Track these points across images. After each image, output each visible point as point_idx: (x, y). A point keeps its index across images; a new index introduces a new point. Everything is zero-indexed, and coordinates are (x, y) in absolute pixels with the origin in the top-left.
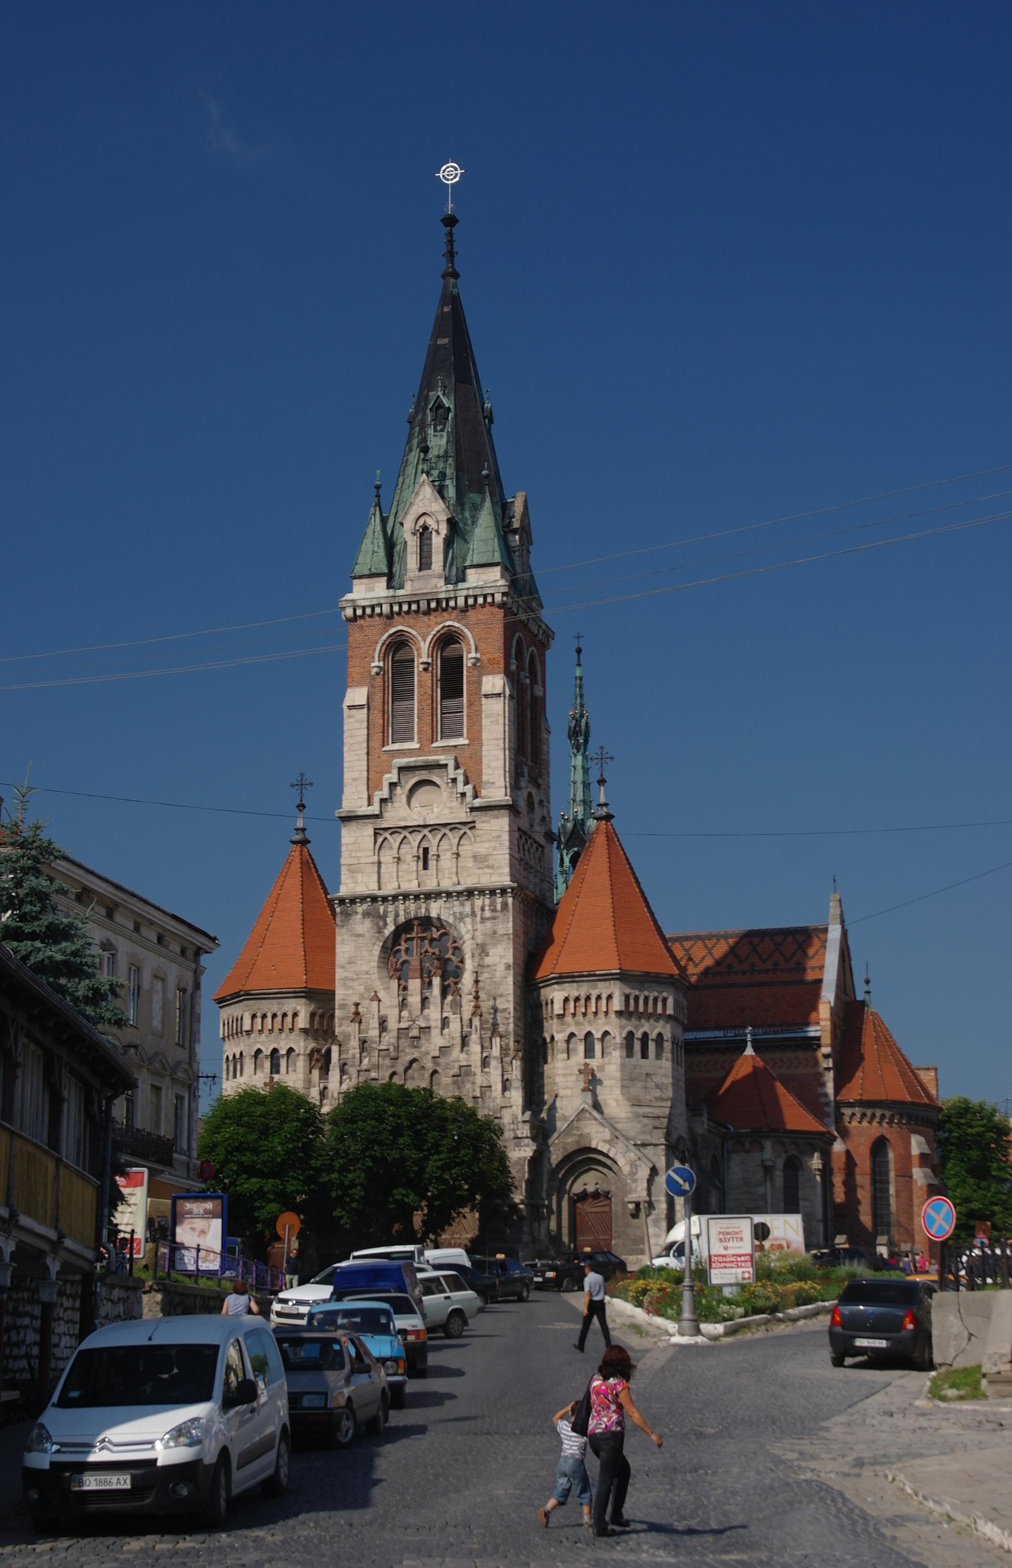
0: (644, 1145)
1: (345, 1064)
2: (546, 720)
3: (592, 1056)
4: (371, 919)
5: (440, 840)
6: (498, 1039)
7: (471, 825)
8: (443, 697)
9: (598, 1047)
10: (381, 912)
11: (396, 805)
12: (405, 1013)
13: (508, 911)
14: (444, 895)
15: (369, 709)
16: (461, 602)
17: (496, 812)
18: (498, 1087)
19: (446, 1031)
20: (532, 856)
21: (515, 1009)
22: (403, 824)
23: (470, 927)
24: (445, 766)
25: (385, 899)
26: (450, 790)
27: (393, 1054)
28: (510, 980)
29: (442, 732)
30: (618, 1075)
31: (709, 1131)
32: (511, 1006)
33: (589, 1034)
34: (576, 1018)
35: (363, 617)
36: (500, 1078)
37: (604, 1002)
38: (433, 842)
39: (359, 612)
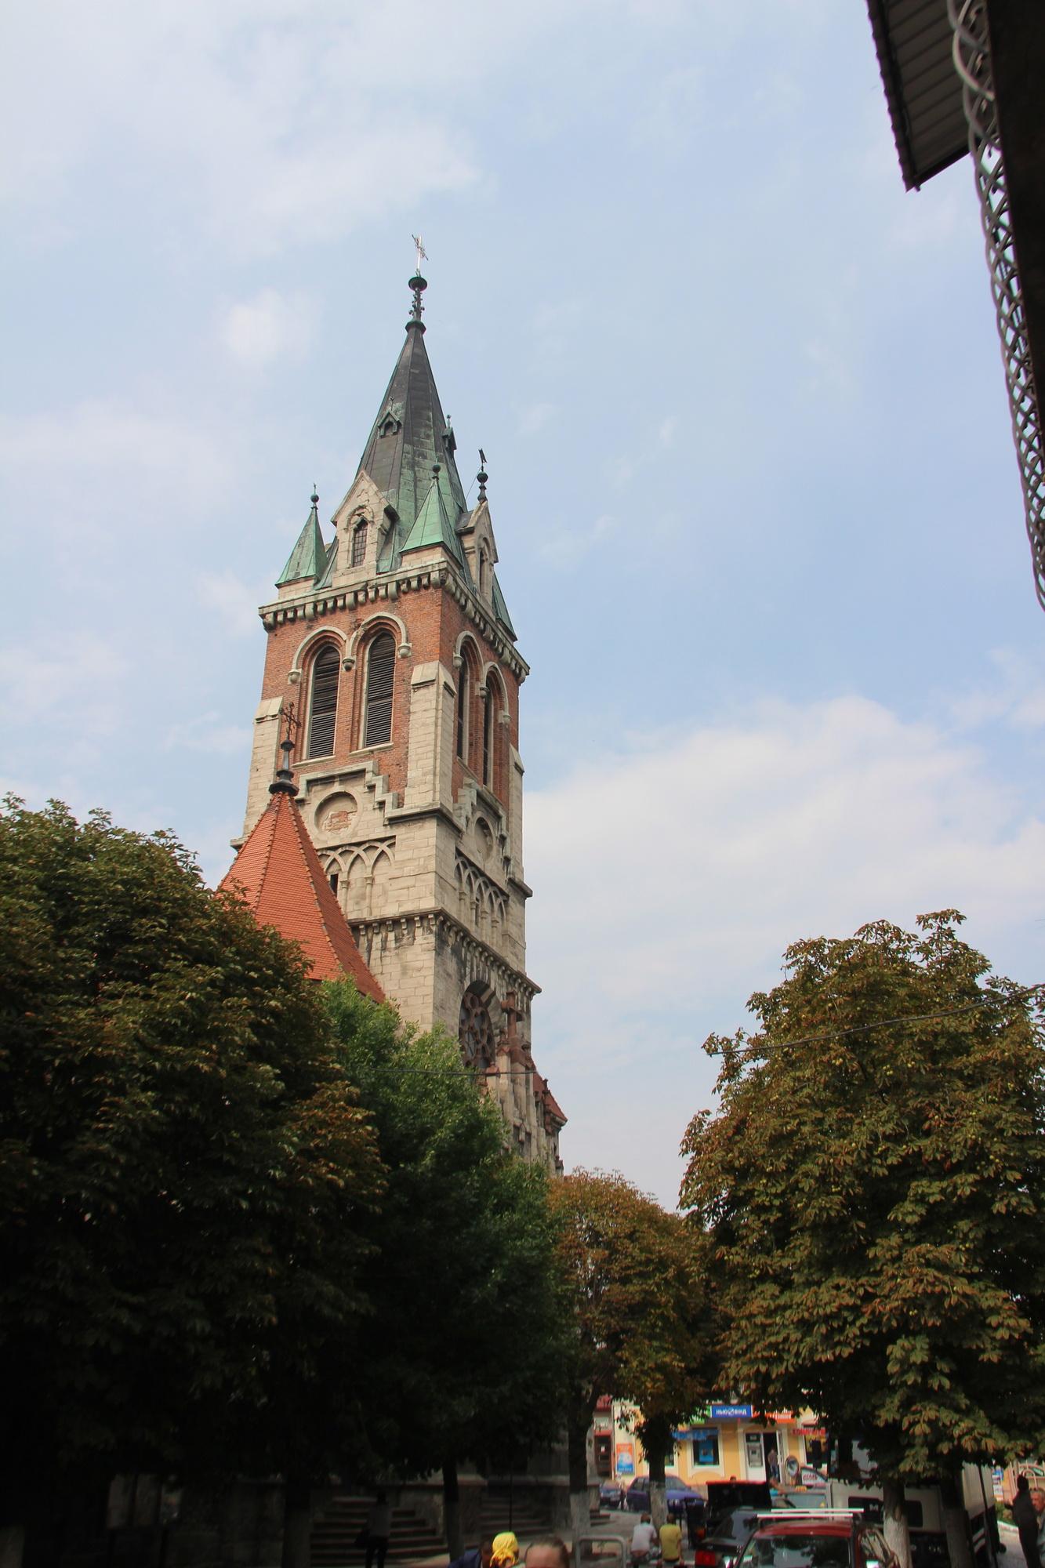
5: (352, 864)
7: (390, 840)
16: (392, 588)
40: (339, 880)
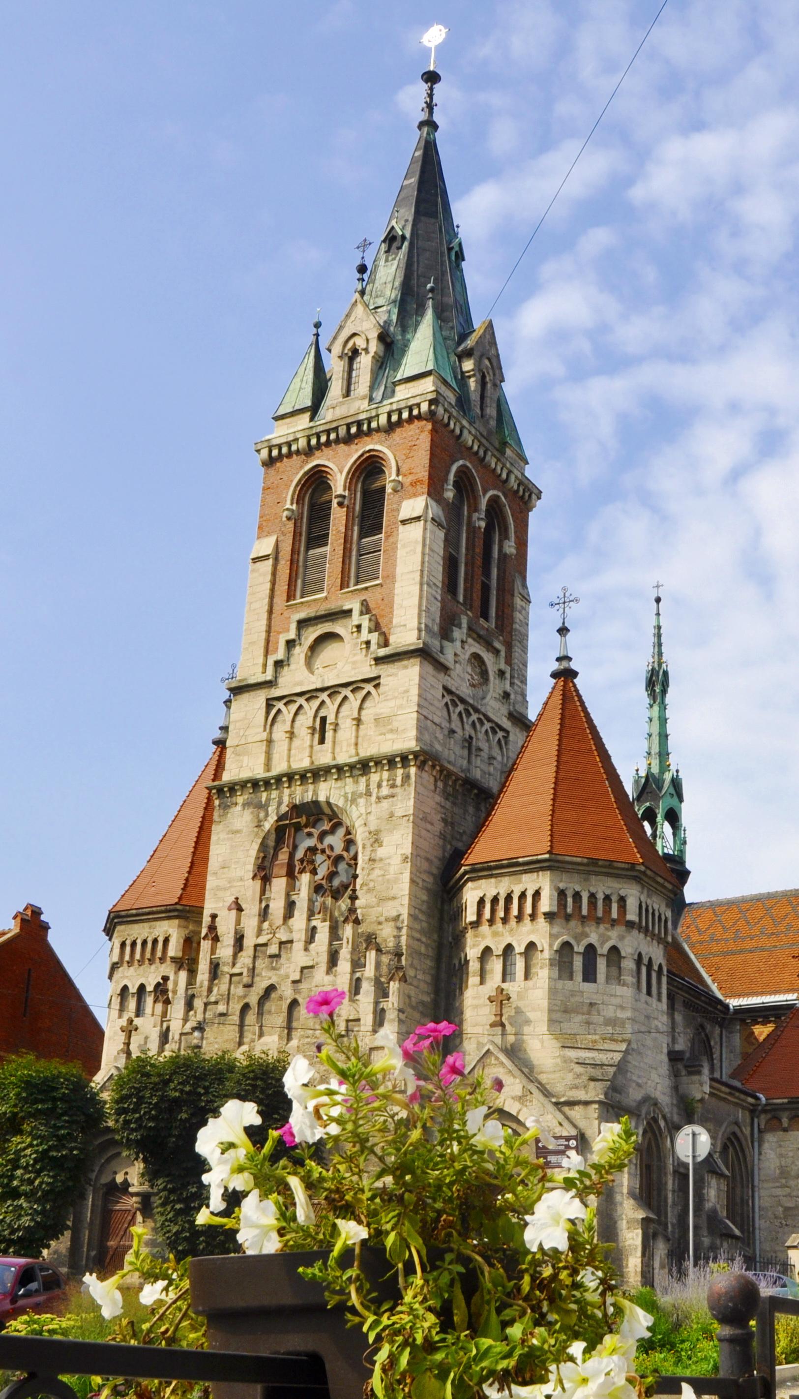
0: (571, 1104)
1: (193, 996)
2: (524, 586)
3: (514, 981)
4: (251, 810)
5: (340, 705)
6: (373, 953)
7: (375, 680)
8: (361, 536)
9: (520, 964)
10: (264, 799)
11: (292, 667)
12: (266, 925)
13: (409, 785)
14: (334, 771)
15: (276, 560)
16: (383, 419)
17: (405, 663)
18: (368, 1020)
19: (313, 945)
20: (481, 736)
21: (410, 915)
22: (298, 690)
23: (362, 810)
24: (349, 612)
25: (267, 783)
26: (354, 641)
27: (246, 979)
28: (406, 877)
29: (357, 577)
30: (545, 1004)
31: (711, 1094)
32: (405, 912)
33: (509, 948)
34: (494, 927)
35: (280, 456)
36: (371, 1008)
37: (529, 900)
38: (329, 712)
39: (275, 453)
40: (328, 722)
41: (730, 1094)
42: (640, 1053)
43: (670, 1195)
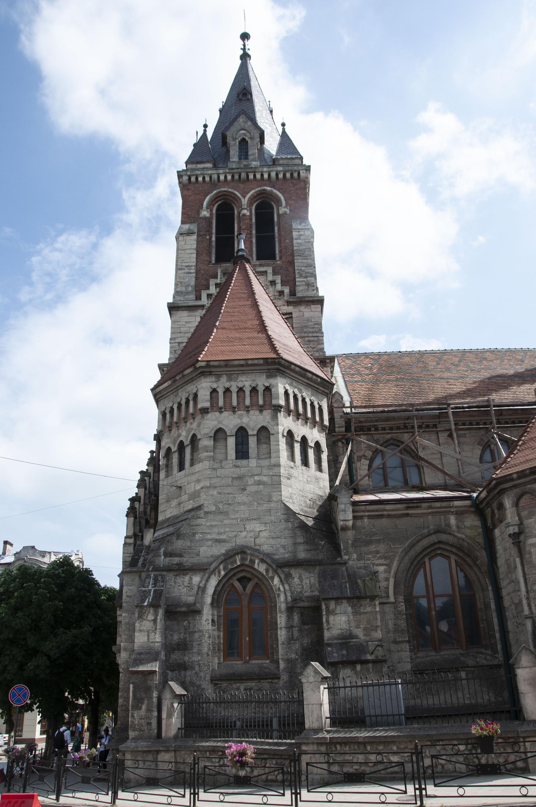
41: (408, 508)
42: (226, 513)
43: (282, 634)
